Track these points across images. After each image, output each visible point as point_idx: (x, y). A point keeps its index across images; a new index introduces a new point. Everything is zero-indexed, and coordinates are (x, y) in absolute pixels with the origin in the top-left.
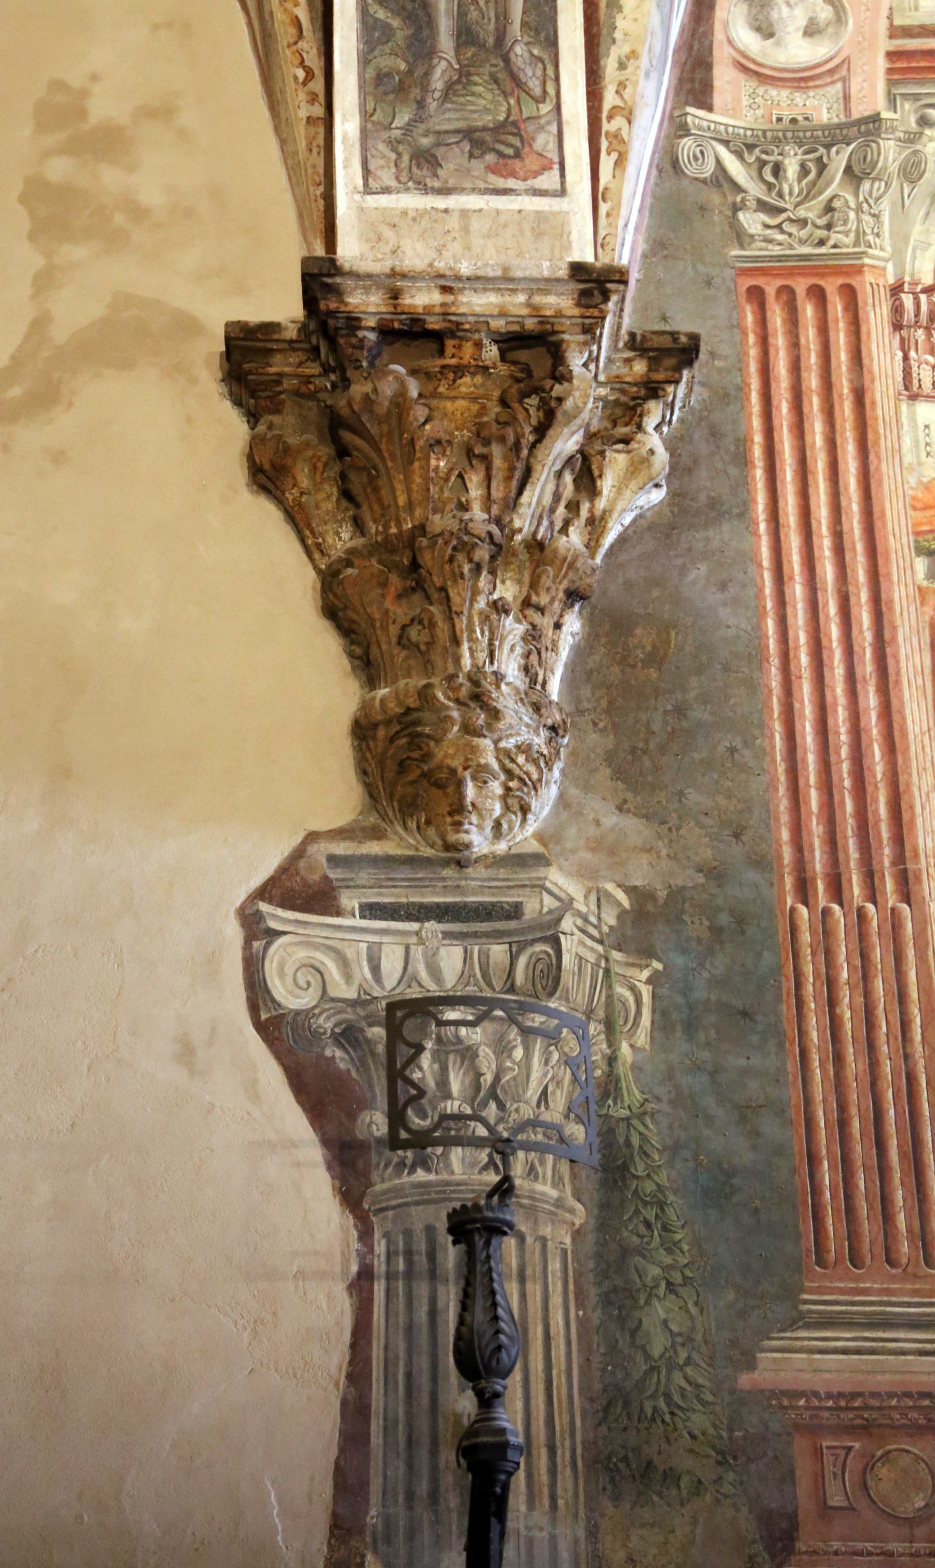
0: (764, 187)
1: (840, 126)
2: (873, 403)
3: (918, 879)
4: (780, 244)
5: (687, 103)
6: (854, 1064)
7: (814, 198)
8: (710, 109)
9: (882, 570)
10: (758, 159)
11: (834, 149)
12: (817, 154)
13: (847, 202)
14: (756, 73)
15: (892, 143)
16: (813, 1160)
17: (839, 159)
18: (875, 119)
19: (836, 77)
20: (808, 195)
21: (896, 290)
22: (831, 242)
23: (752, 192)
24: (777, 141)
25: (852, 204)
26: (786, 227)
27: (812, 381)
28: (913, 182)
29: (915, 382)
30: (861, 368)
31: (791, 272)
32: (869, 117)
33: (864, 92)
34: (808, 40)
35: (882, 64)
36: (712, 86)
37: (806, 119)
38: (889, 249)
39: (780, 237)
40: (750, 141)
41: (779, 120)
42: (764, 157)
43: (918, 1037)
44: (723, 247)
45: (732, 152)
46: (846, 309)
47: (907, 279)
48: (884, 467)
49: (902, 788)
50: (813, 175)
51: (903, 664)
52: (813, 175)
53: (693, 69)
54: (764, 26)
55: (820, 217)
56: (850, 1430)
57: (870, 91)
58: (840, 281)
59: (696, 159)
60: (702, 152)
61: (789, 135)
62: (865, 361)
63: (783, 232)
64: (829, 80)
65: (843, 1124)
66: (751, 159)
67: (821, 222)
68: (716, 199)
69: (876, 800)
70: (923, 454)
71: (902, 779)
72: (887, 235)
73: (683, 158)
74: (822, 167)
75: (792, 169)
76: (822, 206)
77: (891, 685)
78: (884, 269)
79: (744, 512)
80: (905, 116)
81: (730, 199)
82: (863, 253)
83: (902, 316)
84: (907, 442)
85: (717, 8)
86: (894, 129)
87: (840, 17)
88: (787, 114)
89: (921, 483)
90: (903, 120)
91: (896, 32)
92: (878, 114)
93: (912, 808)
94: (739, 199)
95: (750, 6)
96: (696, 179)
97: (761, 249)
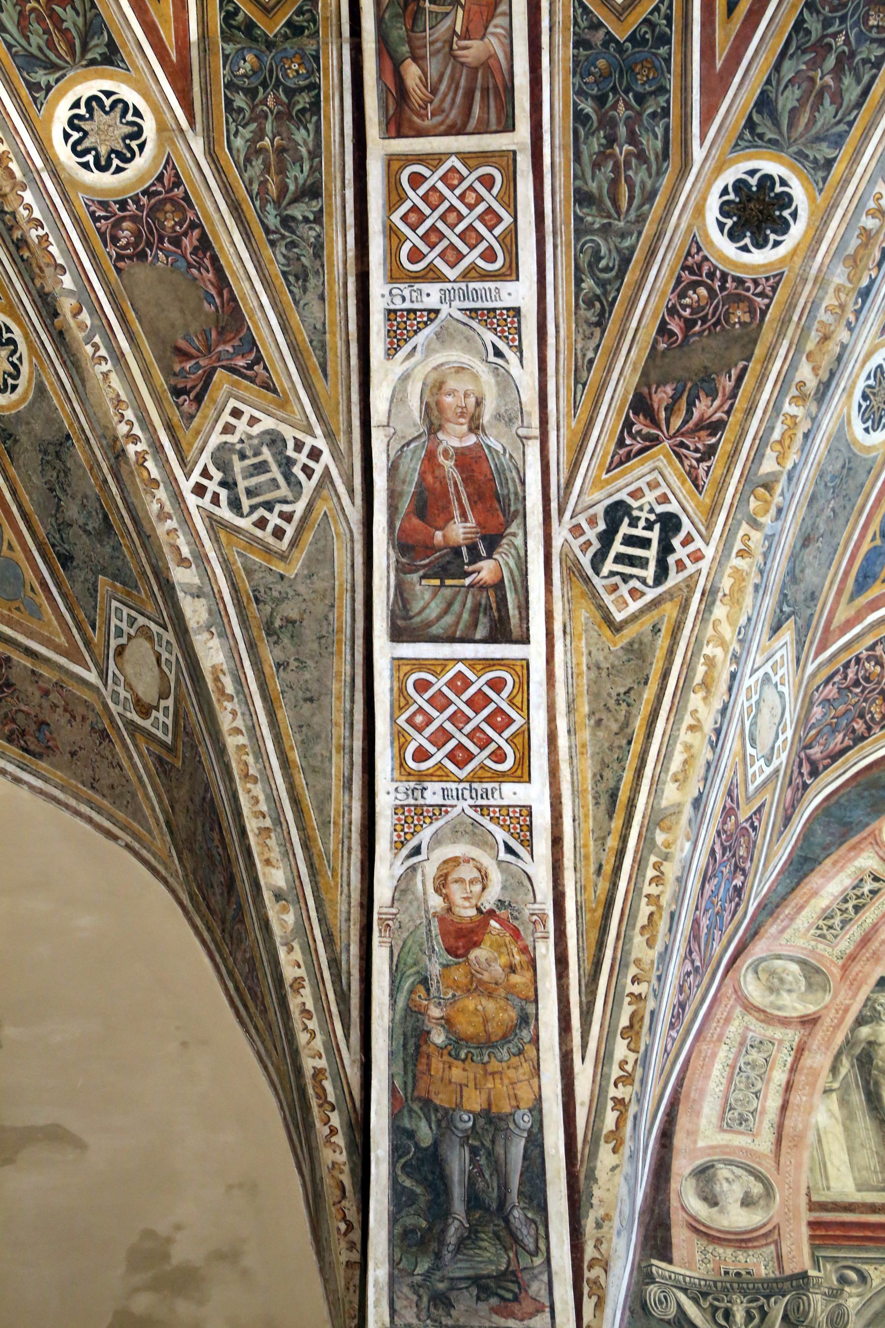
1: (776, 1281)
5: (652, 1256)
8: (670, 1261)
10: (711, 1305)
11: (773, 1300)
12: (759, 1303)
14: (706, 1234)
15: (819, 1297)
18: (804, 1275)
19: (769, 1240)
24: (726, 1291)
32: (798, 1274)
33: (793, 1253)
34: (745, 1209)
35: (805, 1232)
36: (671, 1243)
37: (748, 1273)
40: (704, 1289)
41: (727, 1273)
42: (716, 1303)
50: (757, 1320)
53: (655, 1230)
54: (710, 1197)
57: (798, 1253)
61: (735, 1286)
64: (764, 1242)
66: (706, 1305)
73: (651, 1301)
74: (764, 1314)
80: (827, 1274)
86: (820, 1286)
87: (769, 1191)
90: (827, 1278)
91: (813, 1206)
92: (806, 1272)
95: (698, 1181)
96: (662, 1320)
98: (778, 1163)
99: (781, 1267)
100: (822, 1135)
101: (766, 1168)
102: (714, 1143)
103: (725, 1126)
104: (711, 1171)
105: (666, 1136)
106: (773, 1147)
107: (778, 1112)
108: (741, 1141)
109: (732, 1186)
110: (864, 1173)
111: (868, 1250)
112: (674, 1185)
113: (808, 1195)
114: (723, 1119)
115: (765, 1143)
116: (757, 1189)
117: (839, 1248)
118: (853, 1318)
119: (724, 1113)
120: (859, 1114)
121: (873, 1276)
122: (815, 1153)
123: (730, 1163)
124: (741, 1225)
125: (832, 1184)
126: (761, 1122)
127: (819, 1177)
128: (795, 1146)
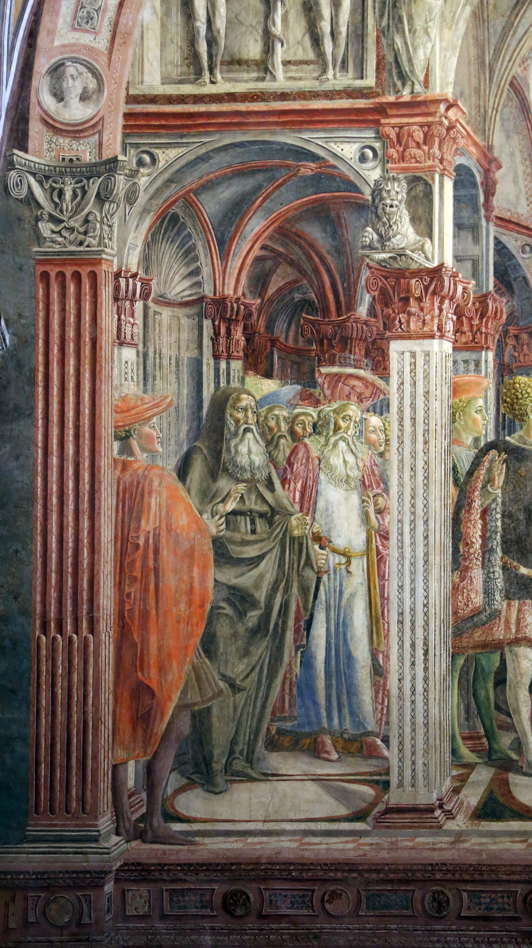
0: (53, 206)
1: (95, 165)
2: (101, 347)
3: (98, 621)
4: (60, 244)
5: (14, 147)
6: (60, 717)
7: (79, 213)
8: (26, 151)
9: (97, 449)
10: (51, 186)
11: (91, 181)
12: (82, 184)
13: (96, 216)
14: (53, 127)
15: (122, 177)
16: (38, 763)
17: (94, 187)
18: (115, 160)
19: (96, 130)
20: (76, 211)
21: (117, 275)
22: (86, 243)
23: (47, 209)
24: (62, 174)
25: (99, 219)
26: (64, 233)
27: (71, 333)
28: (131, 204)
29: (123, 334)
30: (96, 325)
31: (64, 262)
32: (111, 159)
33: (110, 141)
34: (82, 103)
35: (121, 121)
36: (28, 135)
37: (78, 159)
38: (116, 248)
39: (60, 239)
40: (47, 174)
41: (63, 159)
42: (54, 185)
43: (90, 703)
44: (29, 245)
45: (37, 181)
46: (91, 287)
47: (124, 268)
48: (103, 387)
49: (95, 572)
50: (79, 198)
51: (103, 503)
52: (79, 198)
53: (18, 123)
54: (58, 93)
55: (81, 226)
56: (42, 888)
58: (89, 269)
59: (17, 185)
60: (21, 181)
61: (68, 170)
62: (99, 321)
63: (61, 236)
64: (91, 132)
65: (53, 746)
66: (47, 186)
67: (81, 230)
68: (27, 213)
69: (82, 580)
70: (123, 379)
71: (96, 567)
72: (115, 239)
73: (11, 183)
74: (84, 192)
75: (68, 195)
76: (82, 219)
77: (96, 515)
78: (112, 262)
79: (31, 414)
80: (129, 159)
81: (35, 213)
82: (102, 251)
83: (119, 293)
84: (116, 371)
85: (33, 79)
86: (124, 168)
87: (100, 89)
88: (68, 155)
89: (121, 396)
90: (130, 161)
92: (117, 157)
93: (99, 583)
94: (39, 213)
95: (51, 78)
96: (17, 199)
97: (49, 247)
98: (110, 59)
99: (100, 153)
100: (145, 32)
101: (100, 66)
102: (66, 42)
103: (76, 26)
104: (63, 68)
105: (32, 35)
106: (108, 44)
107: (116, 10)
108: (86, 39)
109: (76, 81)
110: (169, 67)
111: (160, 136)
112: (35, 83)
113: (127, 89)
114: (75, 18)
115: (101, 43)
116: (92, 84)
117: (140, 136)
118: (141, 194)
119: (76, 12)
120: (174, 9)
121: (161, 159)
122: (137, 50)
123: (75, 60)
124: (77, 118)
125: (146, 79)
126: (102, 20)
127: (137, 72)
128: (124, 43)
